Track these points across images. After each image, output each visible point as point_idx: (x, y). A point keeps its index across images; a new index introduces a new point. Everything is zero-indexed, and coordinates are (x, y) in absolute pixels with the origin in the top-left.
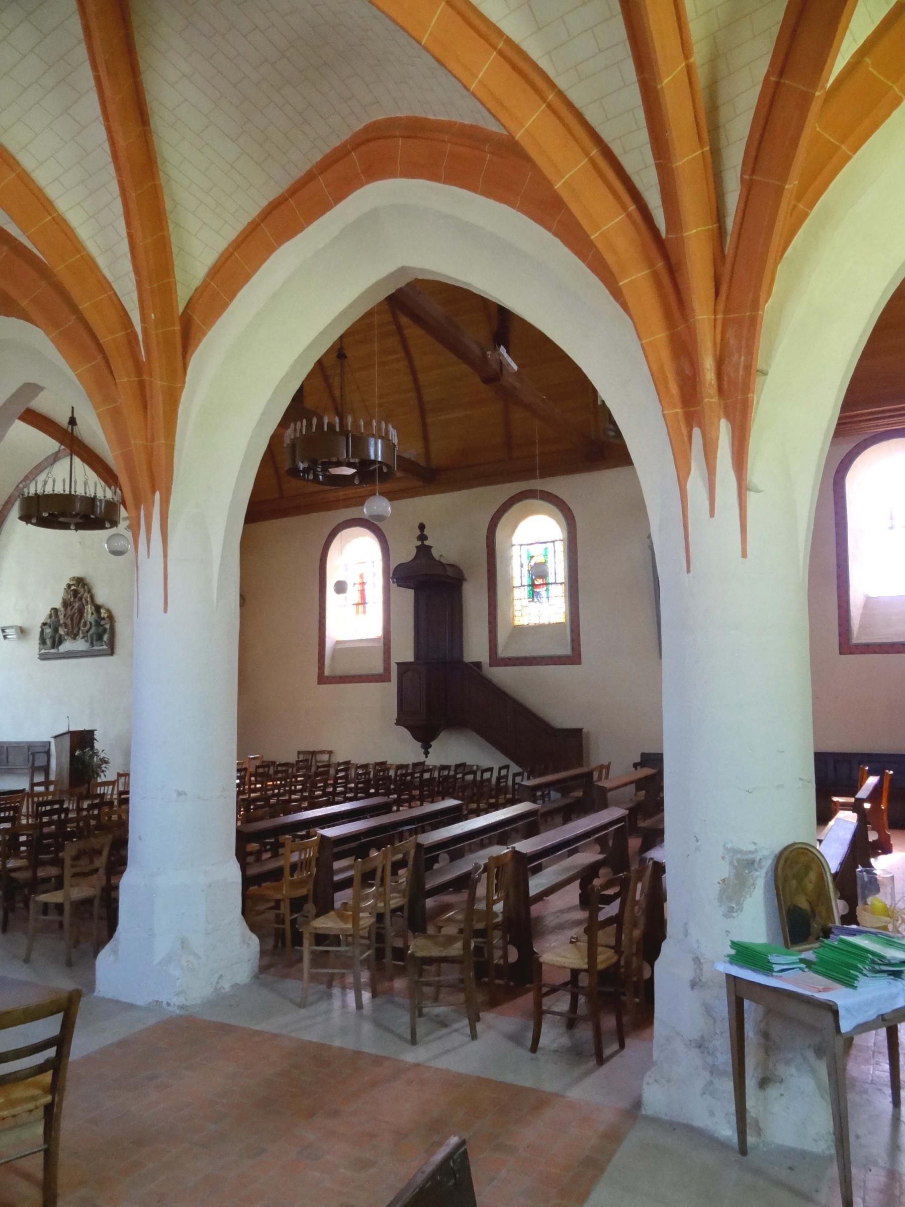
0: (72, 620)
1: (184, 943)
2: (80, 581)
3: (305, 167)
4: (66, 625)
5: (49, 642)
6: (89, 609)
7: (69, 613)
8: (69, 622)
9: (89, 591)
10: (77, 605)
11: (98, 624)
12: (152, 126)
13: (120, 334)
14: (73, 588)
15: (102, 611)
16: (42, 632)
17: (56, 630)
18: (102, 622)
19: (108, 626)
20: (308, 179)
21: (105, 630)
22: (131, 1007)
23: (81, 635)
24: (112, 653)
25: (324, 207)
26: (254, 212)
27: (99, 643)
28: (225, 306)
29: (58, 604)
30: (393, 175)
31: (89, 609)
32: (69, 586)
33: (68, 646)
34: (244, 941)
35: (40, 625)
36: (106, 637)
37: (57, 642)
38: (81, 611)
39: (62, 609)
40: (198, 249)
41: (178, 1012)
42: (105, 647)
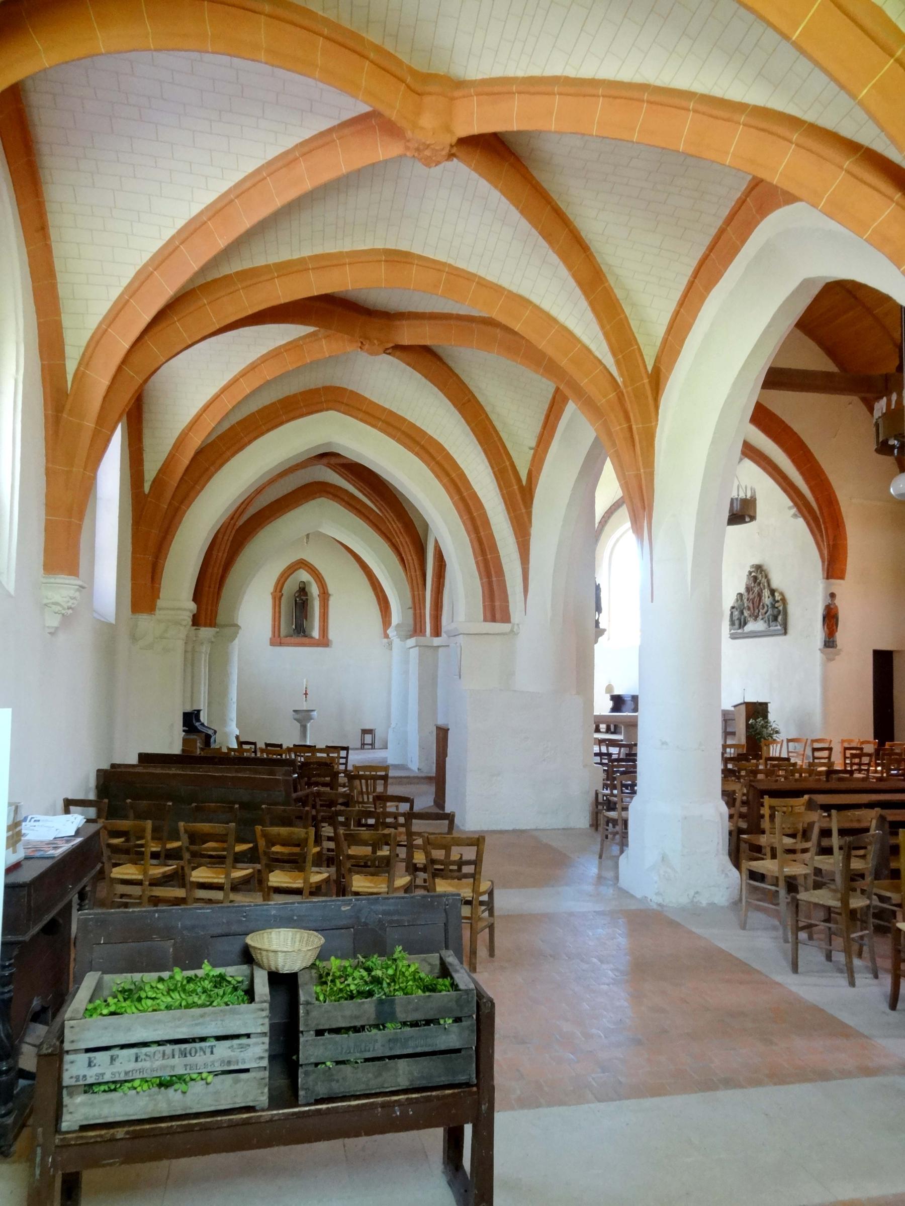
1: (664, 859)
2: (759, 568)
3: (719, 223)
4: (749, 609)
5: (737, 622)
6: (766, 593)
7: (751, 597)
8: (751, 605)
9: (766, 576)
10: (756, 590)
11: (773, 607)
12: (593, 249)
13: (612, 395)
15: (776, 594)
16: (732, 614)
17: (742, 613)
18: (777, 605)
19: (781, 608)
20: (721, 232)
21: (779, 612)
22: (632, 896)
23: (760, 617)
24: (785, 633)
25: (734, 251)
26: (690, 271)
27: (774, 623)
28: (679, 353)
29: (742, 590)
30: (778, 206)
31: (766, 593)
32: (750, 573)
33: (751, 626)
34: (723, 871)
36: (780, 618)
37: (743, 623)
38: (760, 595)
39: (746, 594)
40: (651, 315)
41: (655, 907)
42: (779, 627)
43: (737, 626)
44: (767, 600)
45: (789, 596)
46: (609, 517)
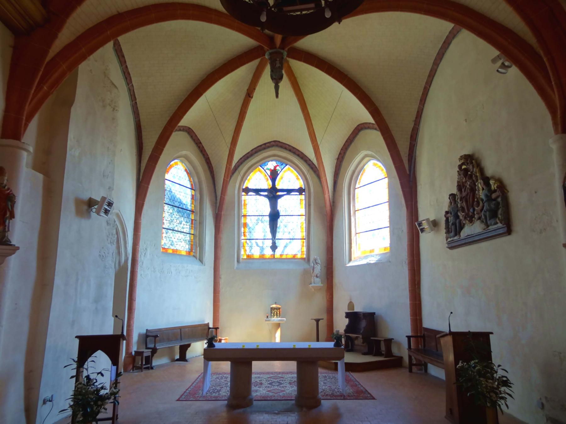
0: (466, 202)
4: (463, 210)
6: (480, 185)
7: (464, 194)
11: (489, 198)
14: (464, 167)
15: (492, 182)
18: (494, 196)
24: (509, 231)
27: (492, 221)
29: (455, 191)
31: (480, 185)
32: (460, 167)
35: (444, 213)
38: (473, 190)
39: (458, 194)
42: (500, 225)
43: (452, 234)
44: (481, 194)
45: (510, 181)
46: (345, 153)
